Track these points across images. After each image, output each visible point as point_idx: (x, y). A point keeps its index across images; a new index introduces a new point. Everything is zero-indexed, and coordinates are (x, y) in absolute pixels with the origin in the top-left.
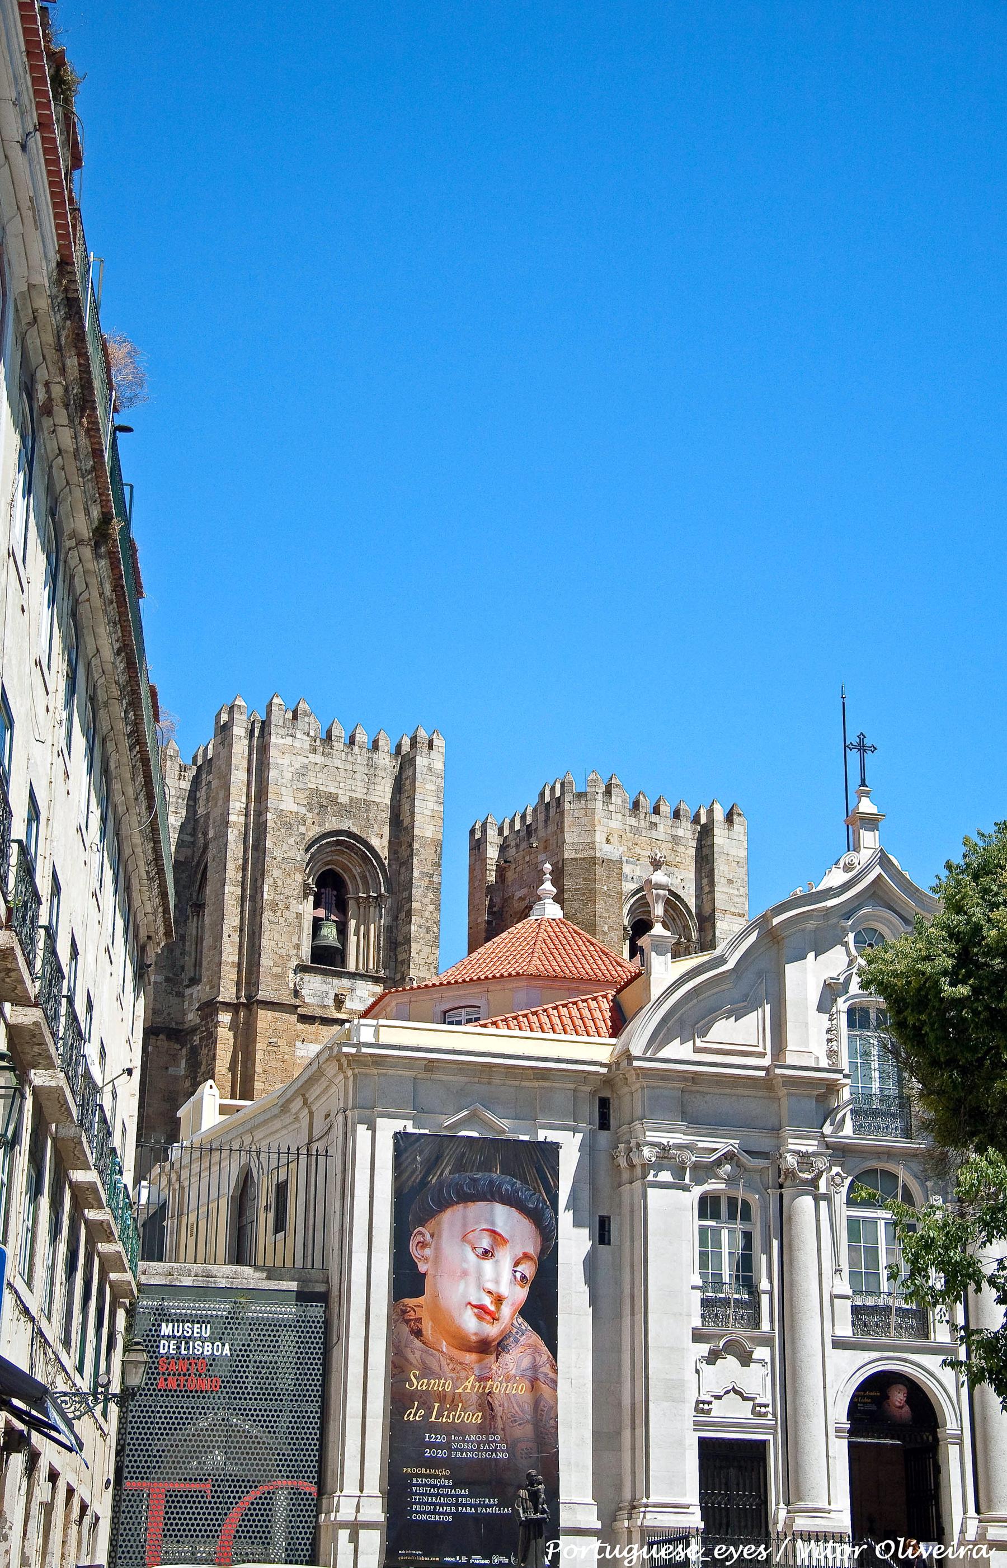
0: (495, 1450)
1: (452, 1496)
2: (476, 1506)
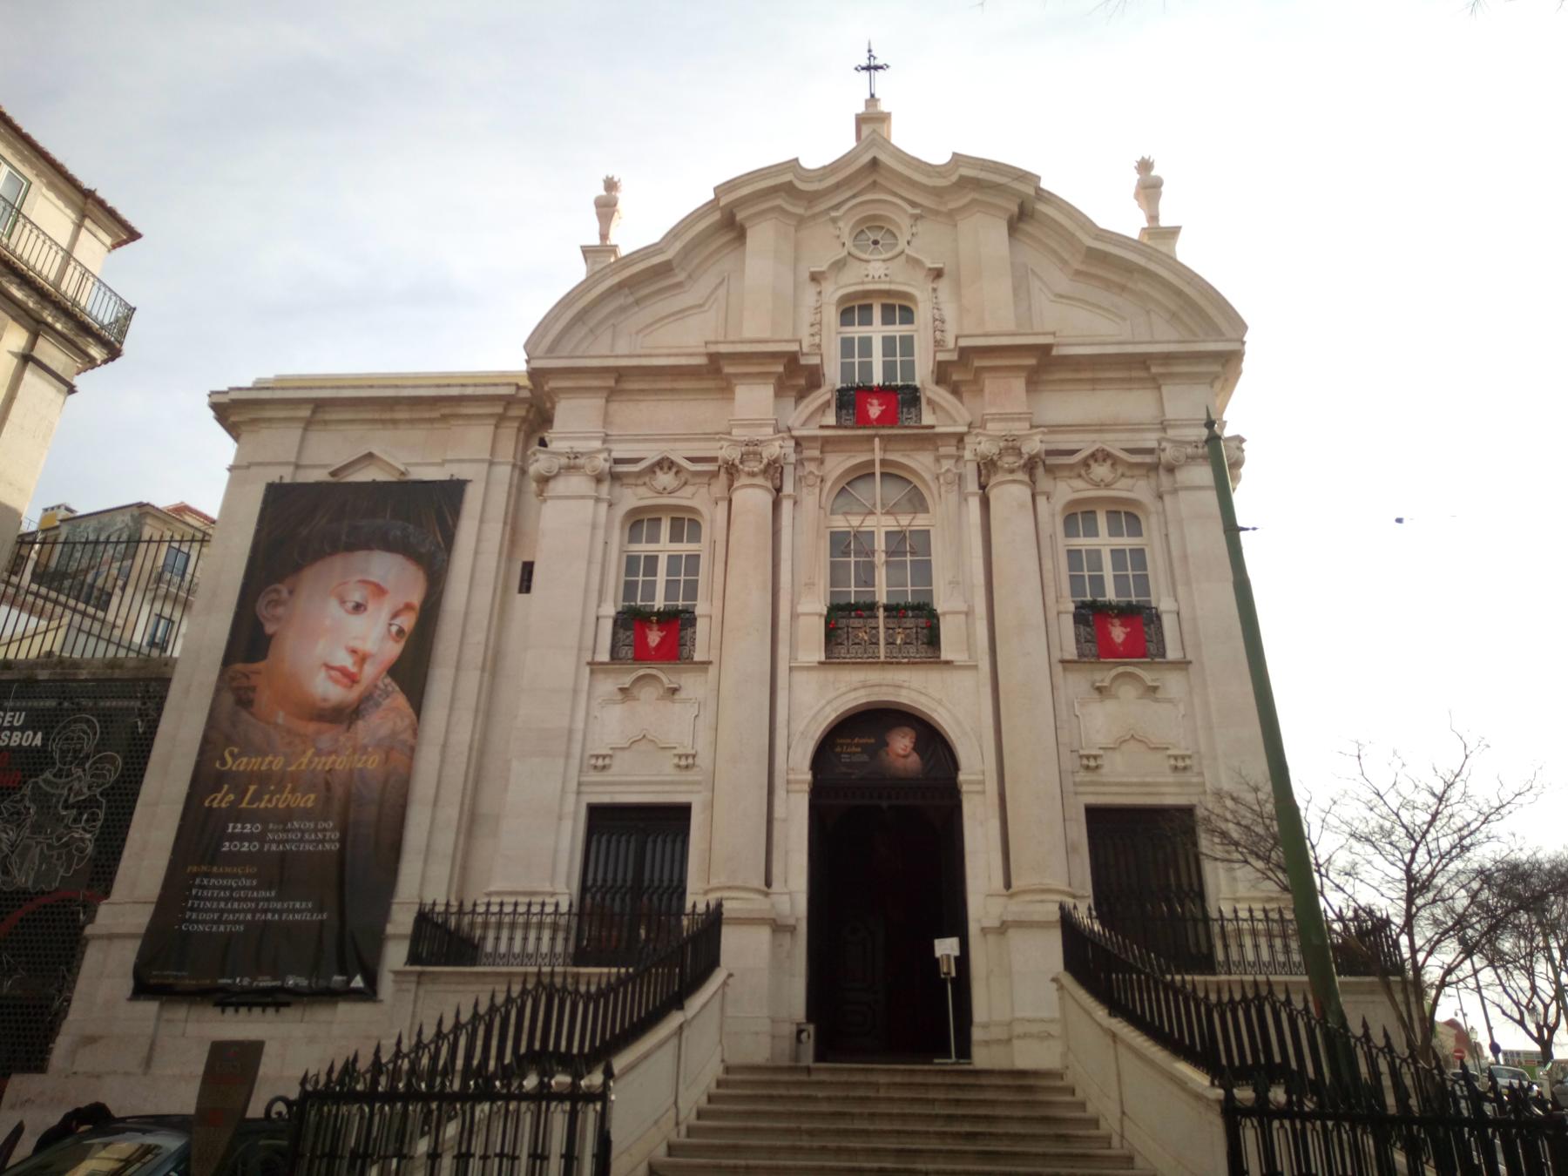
0: (323, 841)
1: (252, 900)
2: (280, 912)
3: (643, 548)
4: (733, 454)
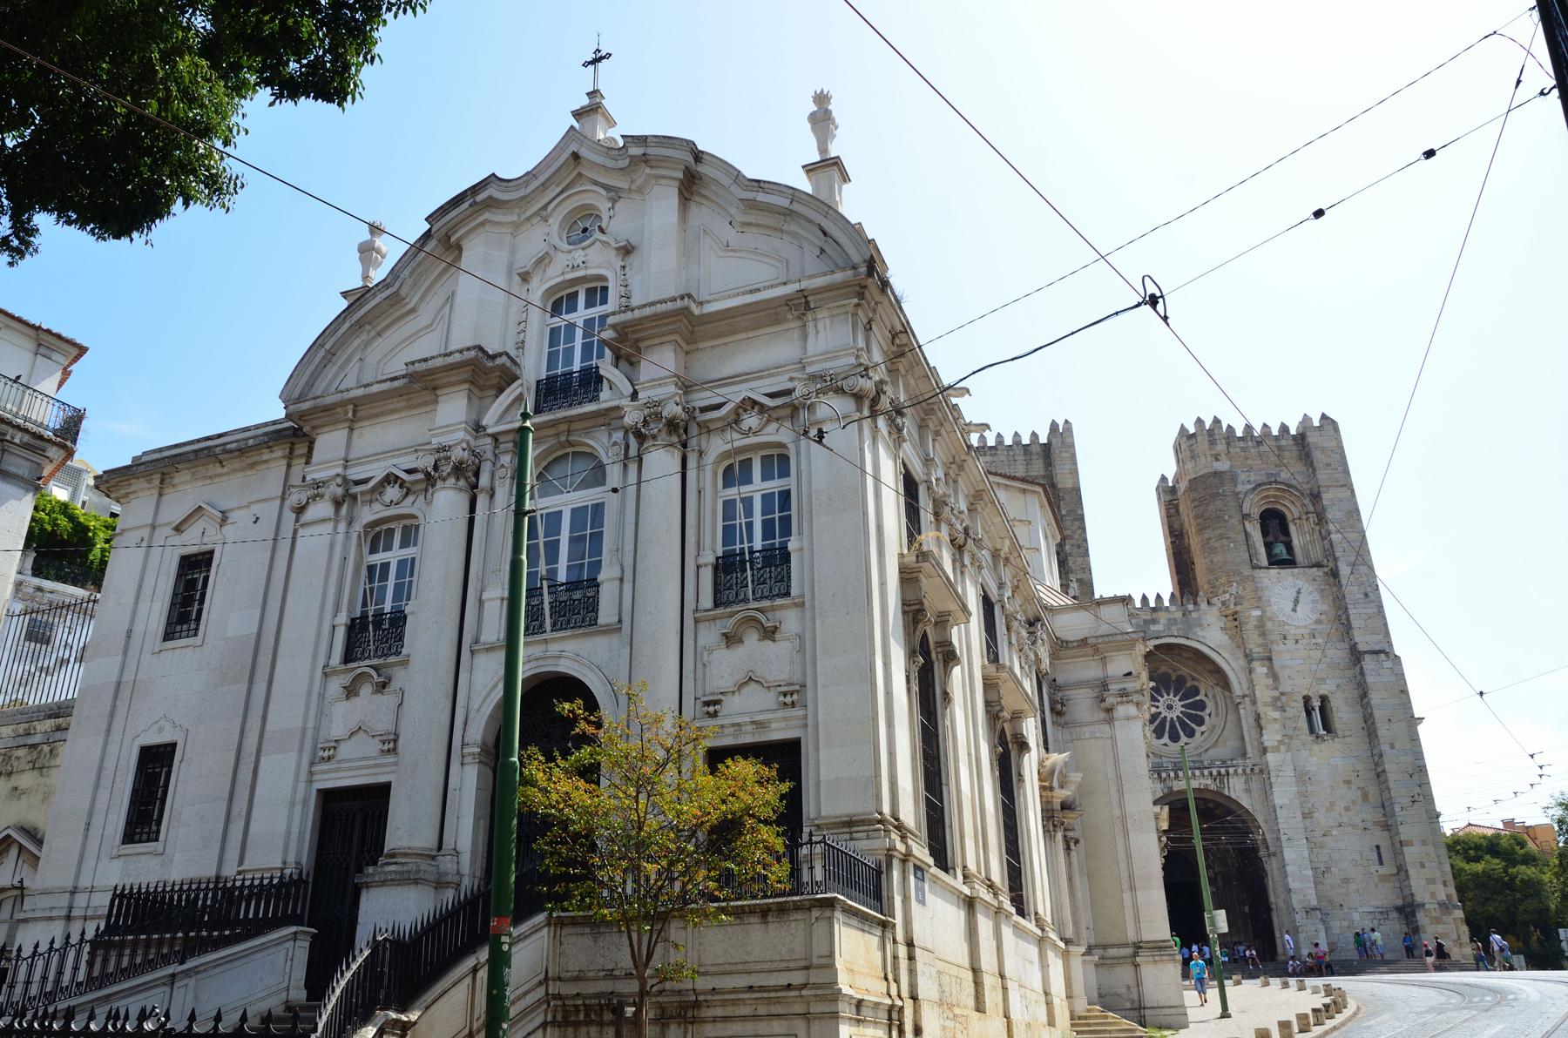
3: (379, 558)
4: (426, 462)
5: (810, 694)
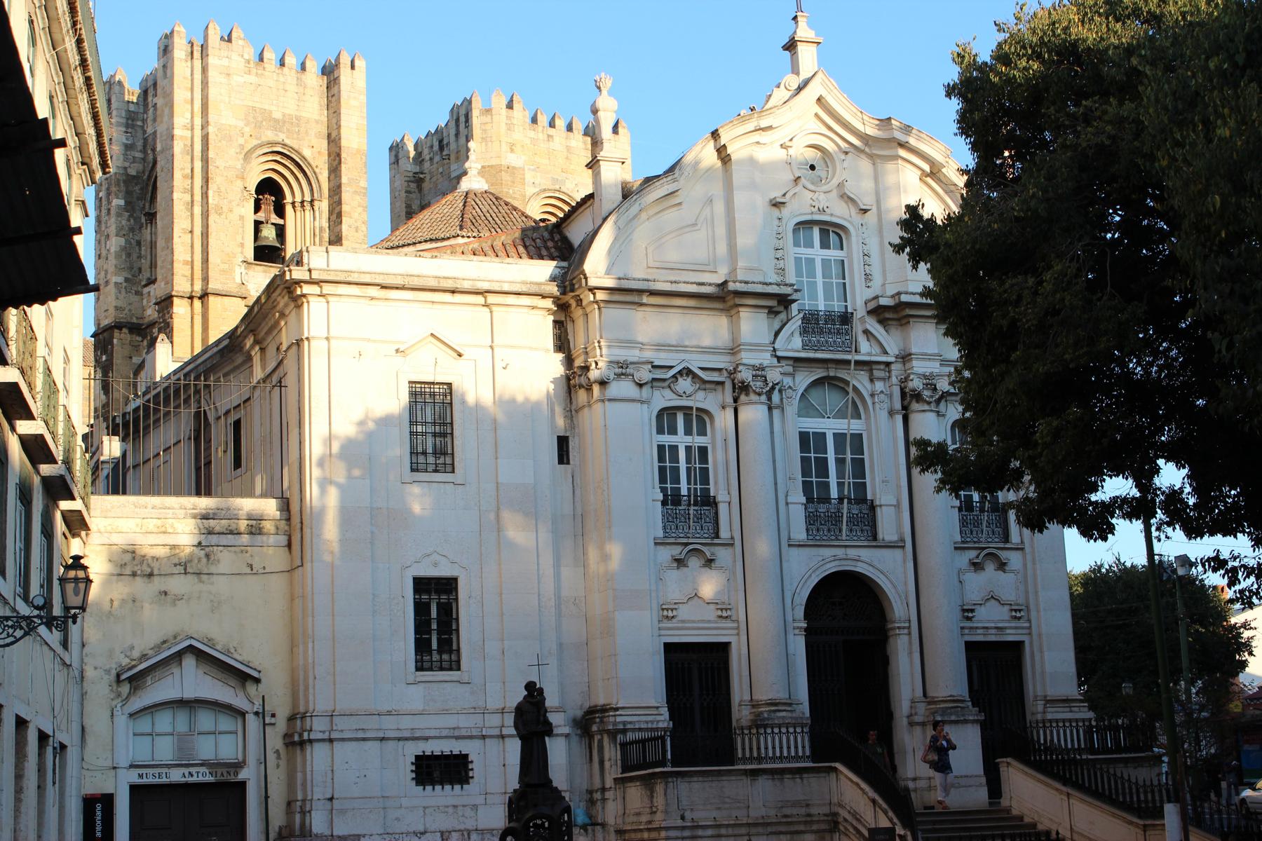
3: (667, 439)
5: (1033, 614)
